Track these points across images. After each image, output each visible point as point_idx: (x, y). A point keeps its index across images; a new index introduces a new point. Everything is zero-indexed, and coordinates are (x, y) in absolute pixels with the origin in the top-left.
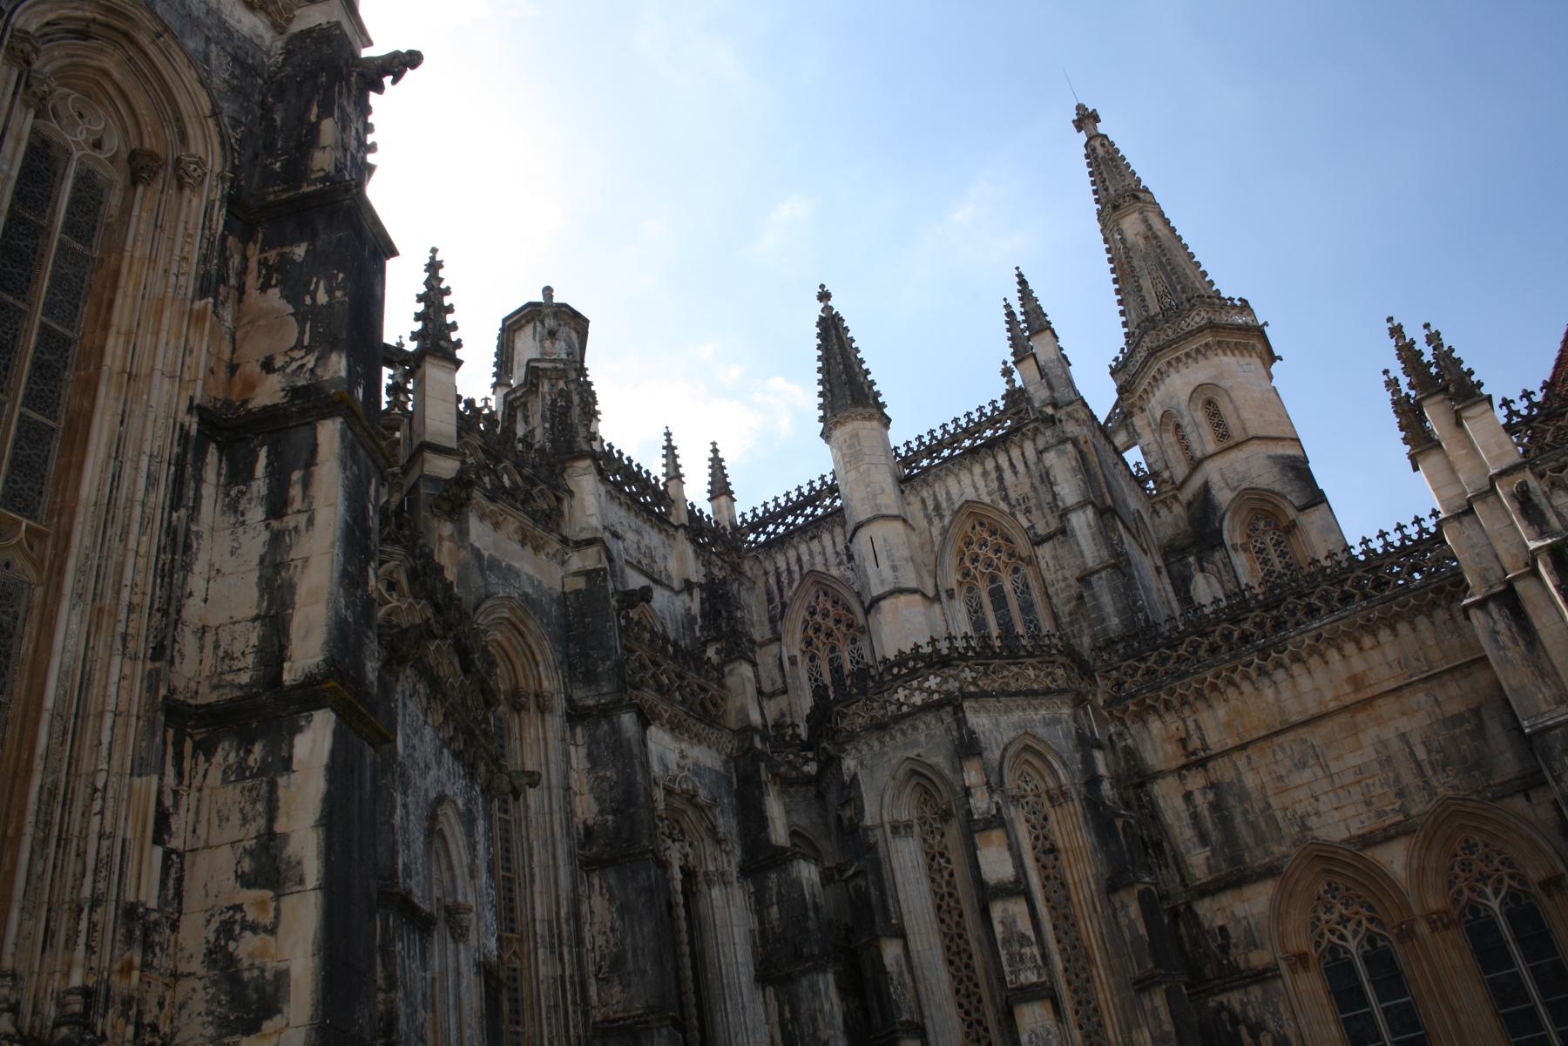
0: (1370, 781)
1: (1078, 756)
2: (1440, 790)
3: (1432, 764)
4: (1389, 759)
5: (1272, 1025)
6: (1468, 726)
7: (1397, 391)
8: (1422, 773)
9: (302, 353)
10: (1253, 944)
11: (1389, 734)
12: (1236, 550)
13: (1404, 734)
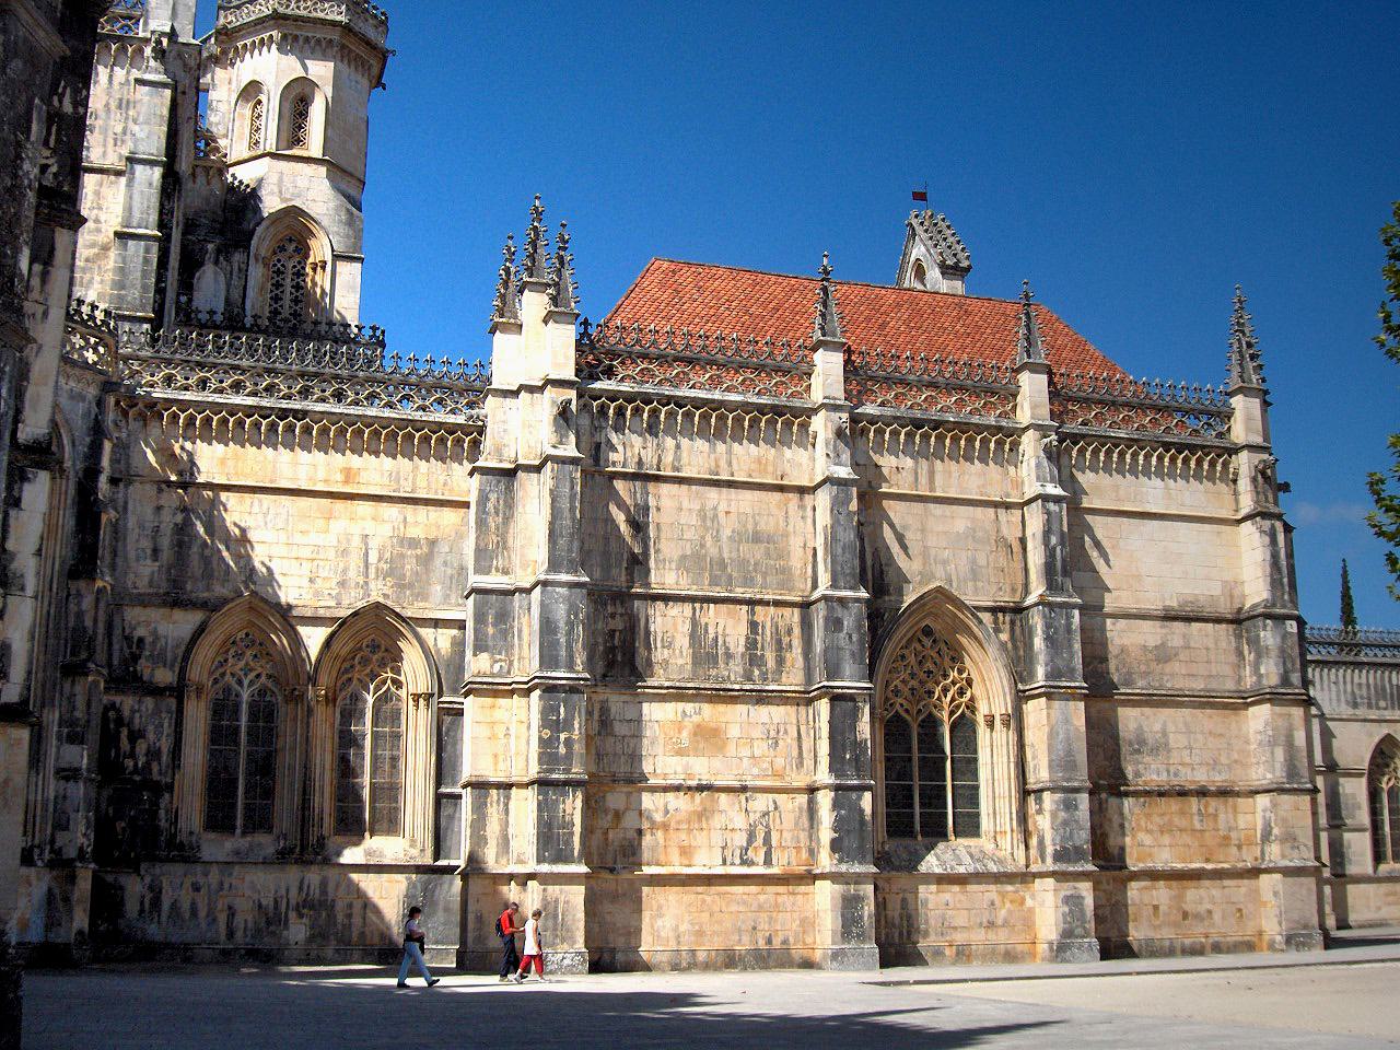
0: (321, 563)
1: (88, 439)
2: (374, 593)
3: (377, 569)
5: (151, 736)
6: (419, 552)
9: (47, 153)
10: (159, 659)
12: (257, 260)
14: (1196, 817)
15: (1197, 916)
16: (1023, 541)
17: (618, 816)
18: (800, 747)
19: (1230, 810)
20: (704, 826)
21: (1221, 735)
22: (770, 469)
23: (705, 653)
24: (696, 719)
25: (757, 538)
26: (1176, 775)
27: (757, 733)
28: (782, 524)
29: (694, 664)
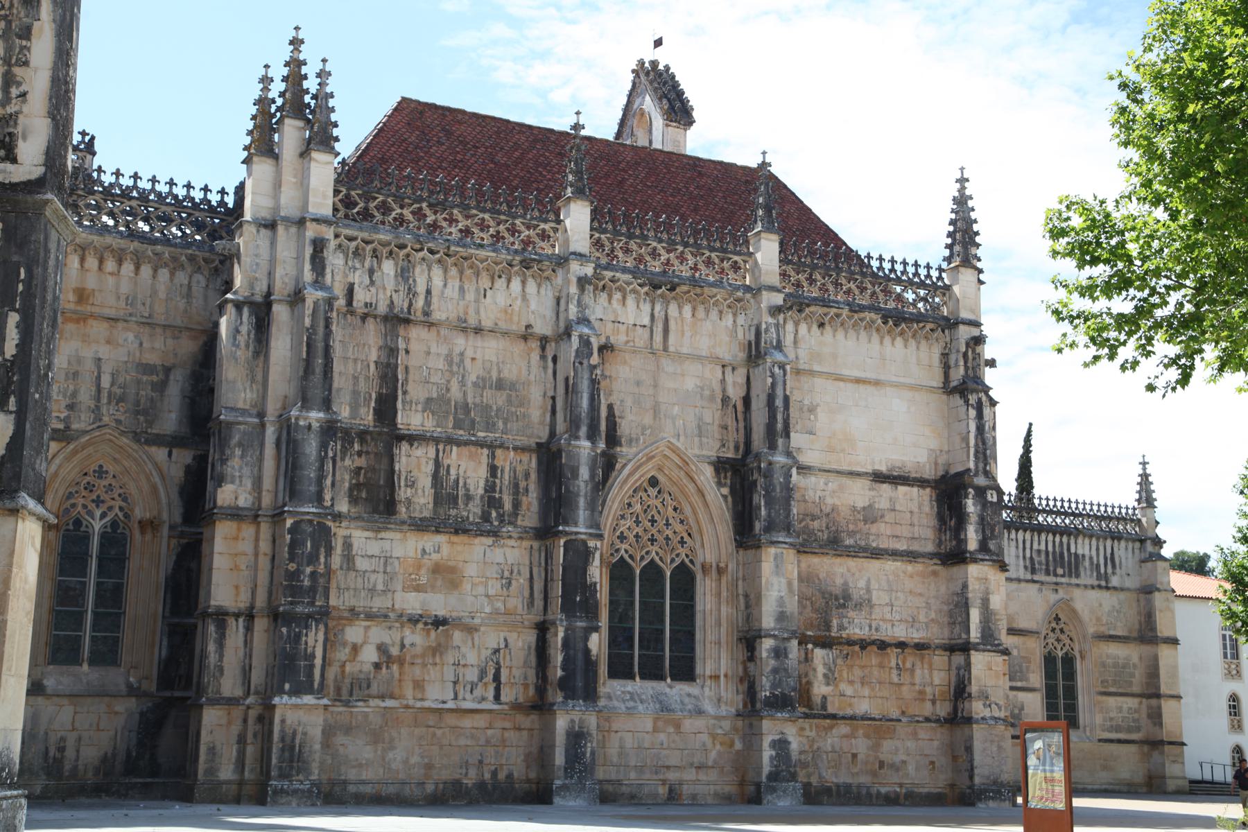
3: (110, 394)
4: (76, 374)
6: (155, 378)
7: (266, 89)
8: (98, 399)
11: (88, 353)
13: (99, 359)
14: (895, 672)
15: (892, 766)
16: (747, 400)
17: (355, 649)
18: (531, 588)
19: (926, 666)
20: (438, 660)
21: (920, 595)
22: (516, 319)
23: (446, 493)
24: (435, 557)
25: (500, 385)
26: (877, 630)
27: (492, 572)
28: (524, 372)
29: (436, 503)
